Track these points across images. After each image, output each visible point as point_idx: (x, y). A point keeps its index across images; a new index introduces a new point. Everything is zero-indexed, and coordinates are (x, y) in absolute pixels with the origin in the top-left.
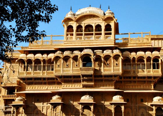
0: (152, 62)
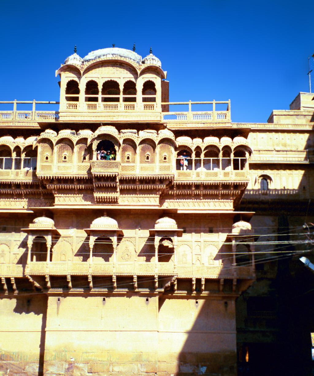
0: (232, 157)
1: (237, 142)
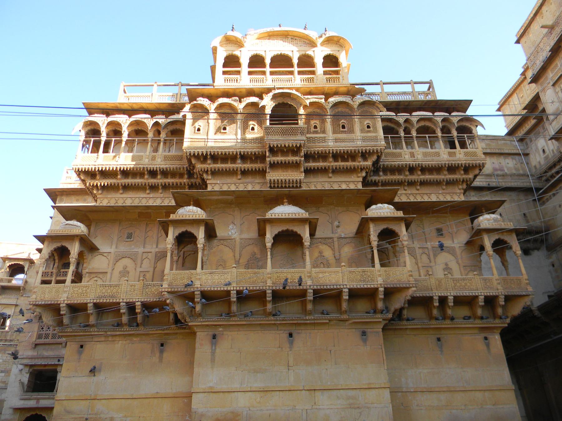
0: (455, 133)
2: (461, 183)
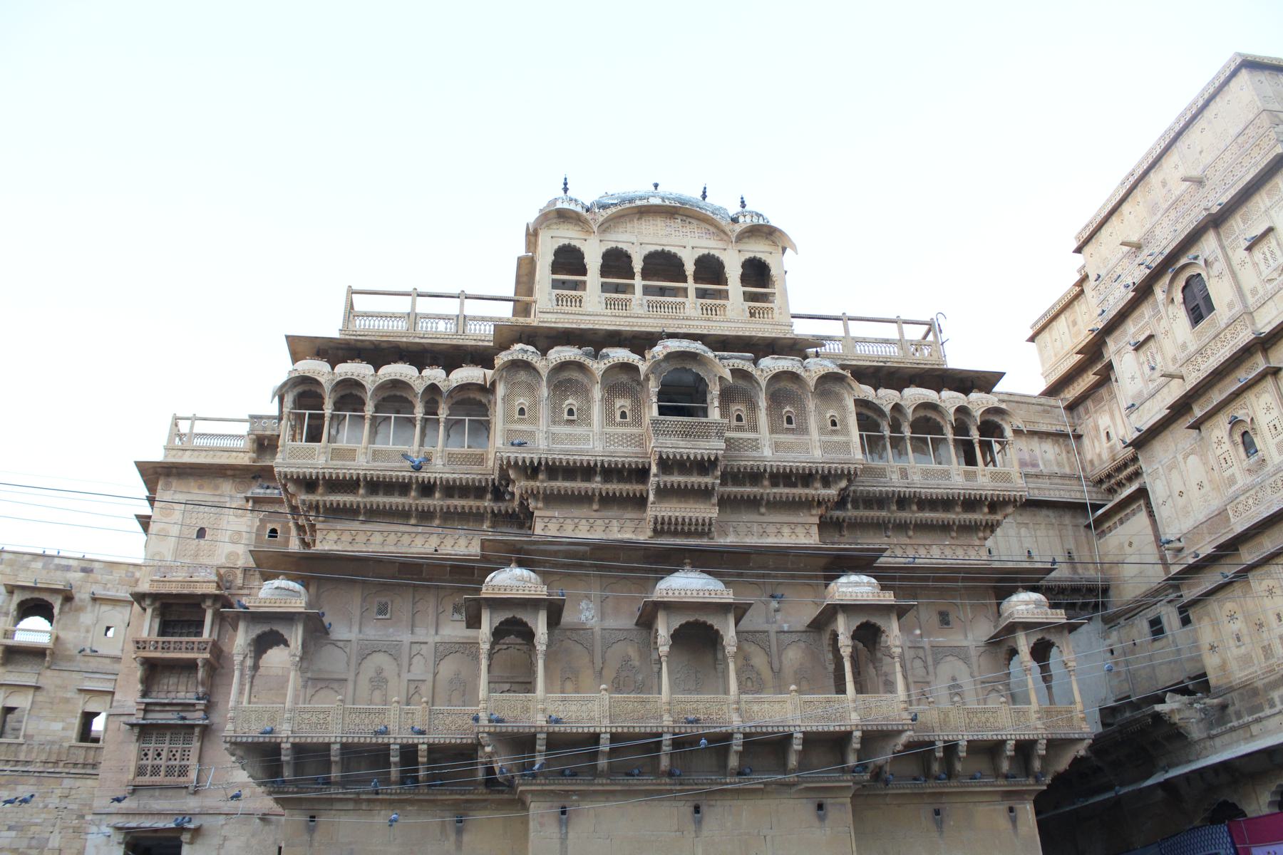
0: (975, 435)
1: (979, 403)
2: (982, 528)
